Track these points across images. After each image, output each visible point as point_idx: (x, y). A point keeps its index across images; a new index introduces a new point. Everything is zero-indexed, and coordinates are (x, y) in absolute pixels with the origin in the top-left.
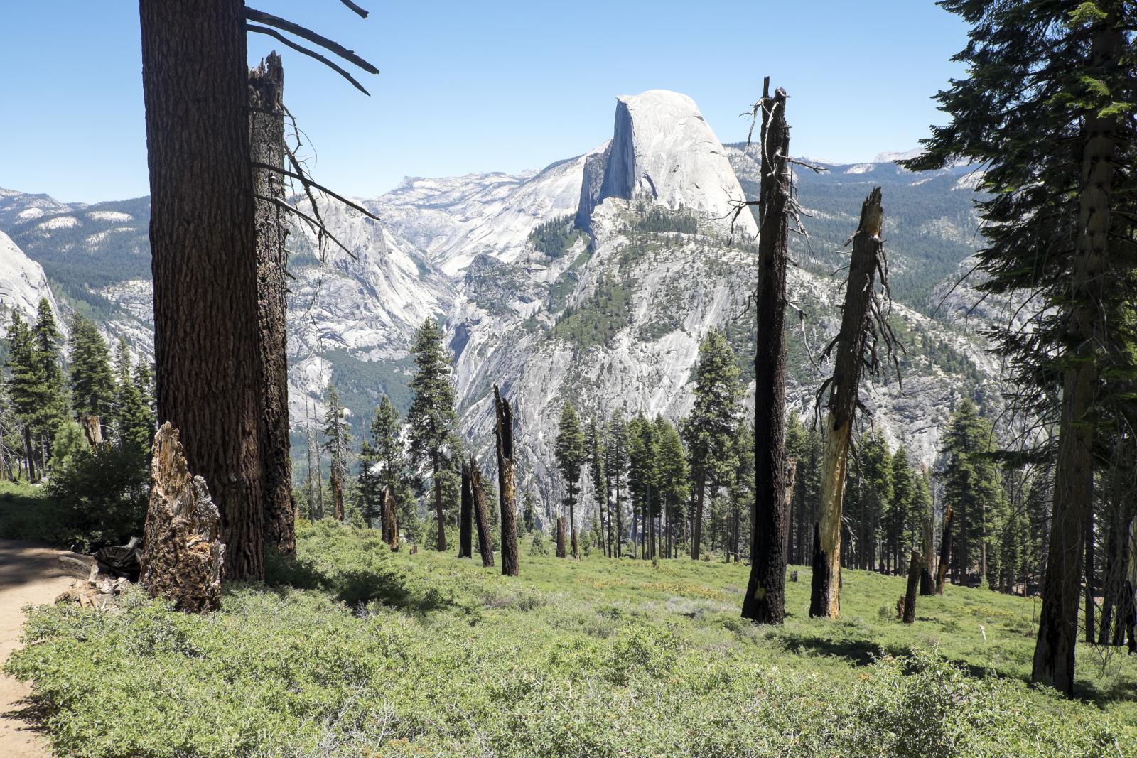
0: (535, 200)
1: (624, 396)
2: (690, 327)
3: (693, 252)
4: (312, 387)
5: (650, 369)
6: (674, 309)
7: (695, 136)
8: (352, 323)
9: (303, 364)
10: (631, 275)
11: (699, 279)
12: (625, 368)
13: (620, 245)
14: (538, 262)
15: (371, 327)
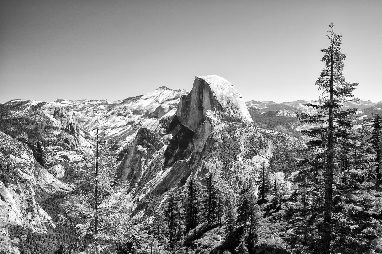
0: (125, 111)
1: (246, 176)
2: (262, 154)
3: (255, 130)
4: (58, 176)
5: (252, 168)
6: (255, 148)
7: (233, 91)
8: (71, 152)
9: (55, 167)
10: (235, 136)
11: (261, 138)
12: (243, 167)
13: (224, 126)
14: (164, 132)
15: (78, 154)
